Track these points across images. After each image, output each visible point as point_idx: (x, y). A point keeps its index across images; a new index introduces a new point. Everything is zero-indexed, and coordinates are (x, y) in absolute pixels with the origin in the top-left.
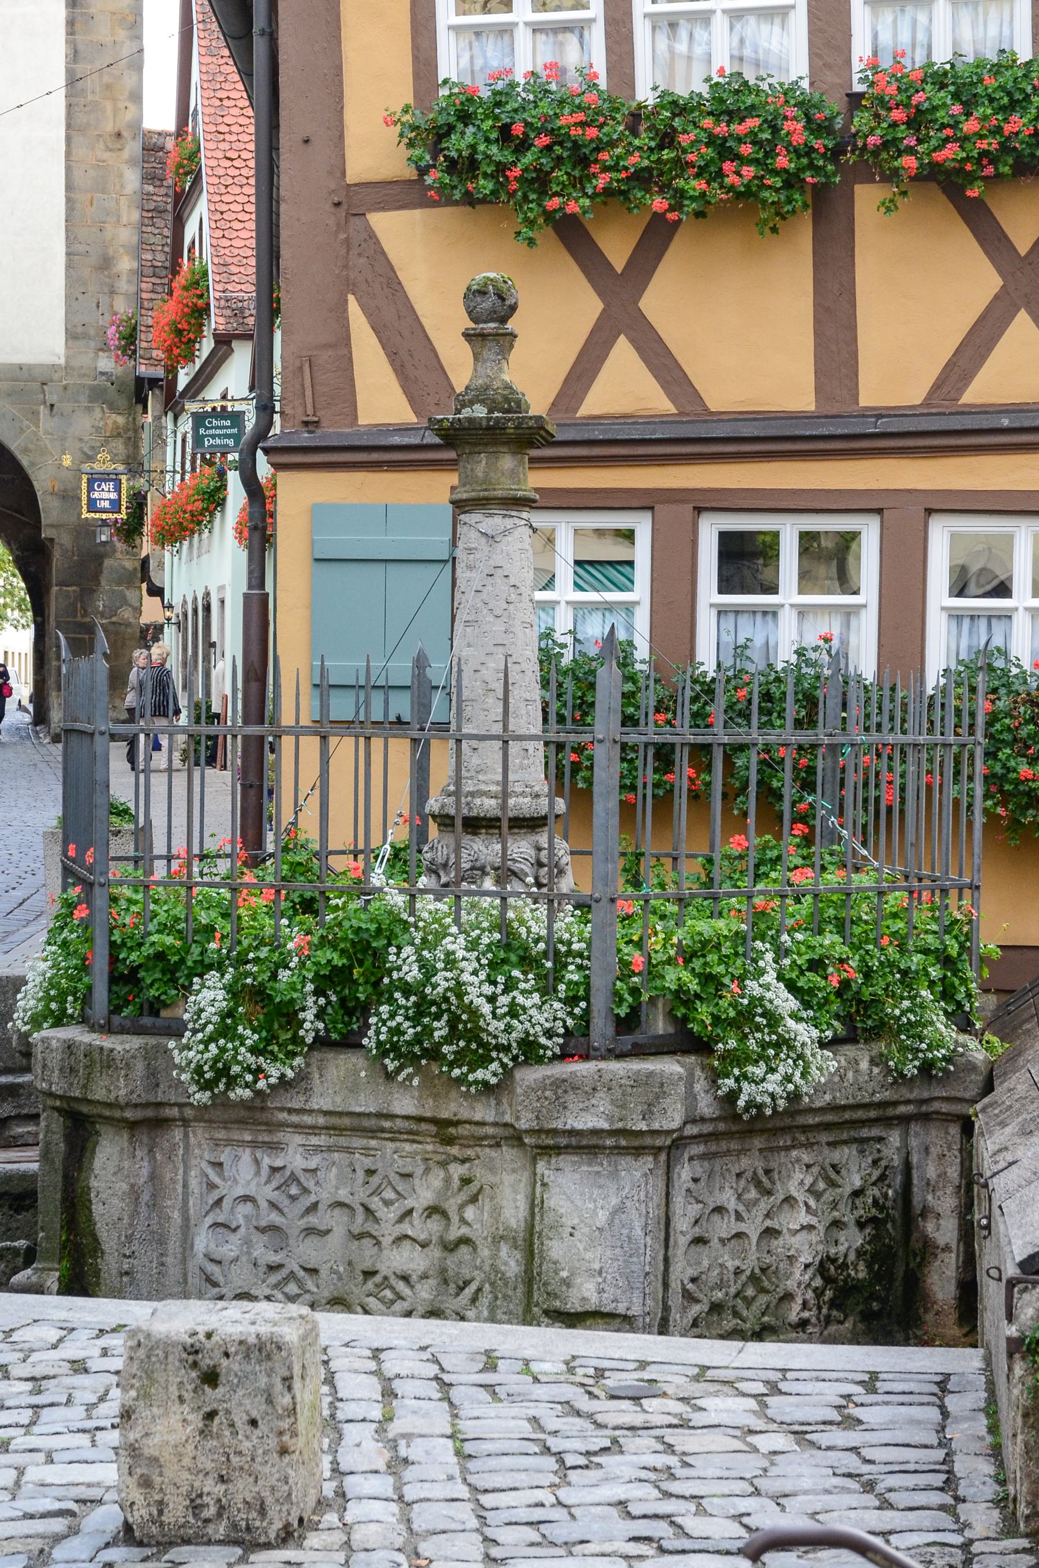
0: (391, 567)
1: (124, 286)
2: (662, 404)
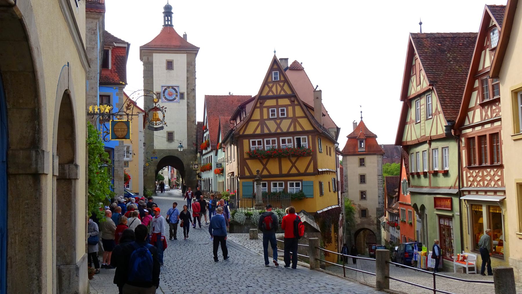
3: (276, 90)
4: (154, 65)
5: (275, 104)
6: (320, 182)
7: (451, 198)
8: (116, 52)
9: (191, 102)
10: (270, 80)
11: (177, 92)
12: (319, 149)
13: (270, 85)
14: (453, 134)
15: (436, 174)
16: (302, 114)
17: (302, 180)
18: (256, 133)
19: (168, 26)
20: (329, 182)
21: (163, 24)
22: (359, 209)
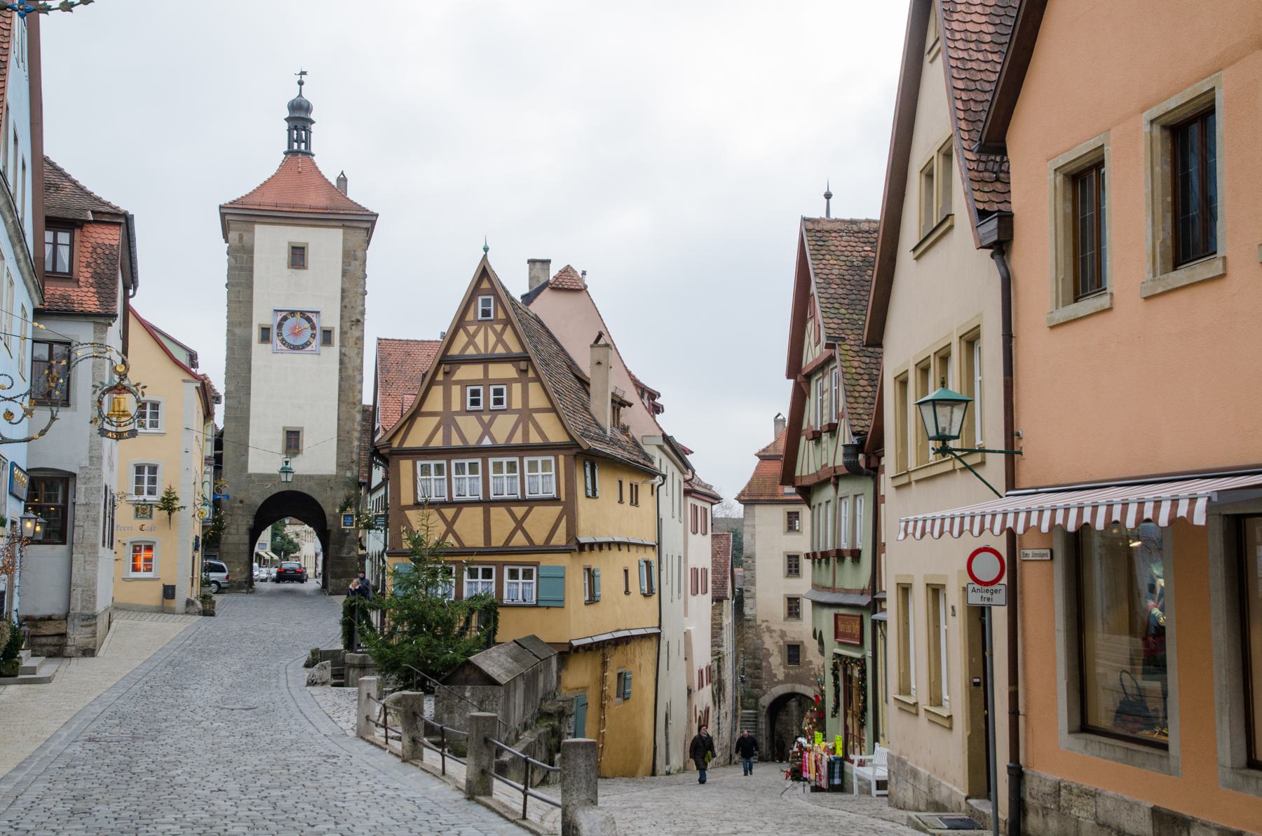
1: (356, 450)
3: (485, 341)
4: (257, 255)
5: (481, 377)
6: (589, 570)
7: (861, 617)
8: (97, 236)
9: (352, 352)
10: (470, 317)
11: (313, 327)
12: (586, 488)
13: (472, 329)
14: (863, 464)
15: (840, 555)
16: (541, 402)
17: (539, 563)
19: (300, 155)
20: (626, 571)
21: (286, 149)
22: (782, 644)
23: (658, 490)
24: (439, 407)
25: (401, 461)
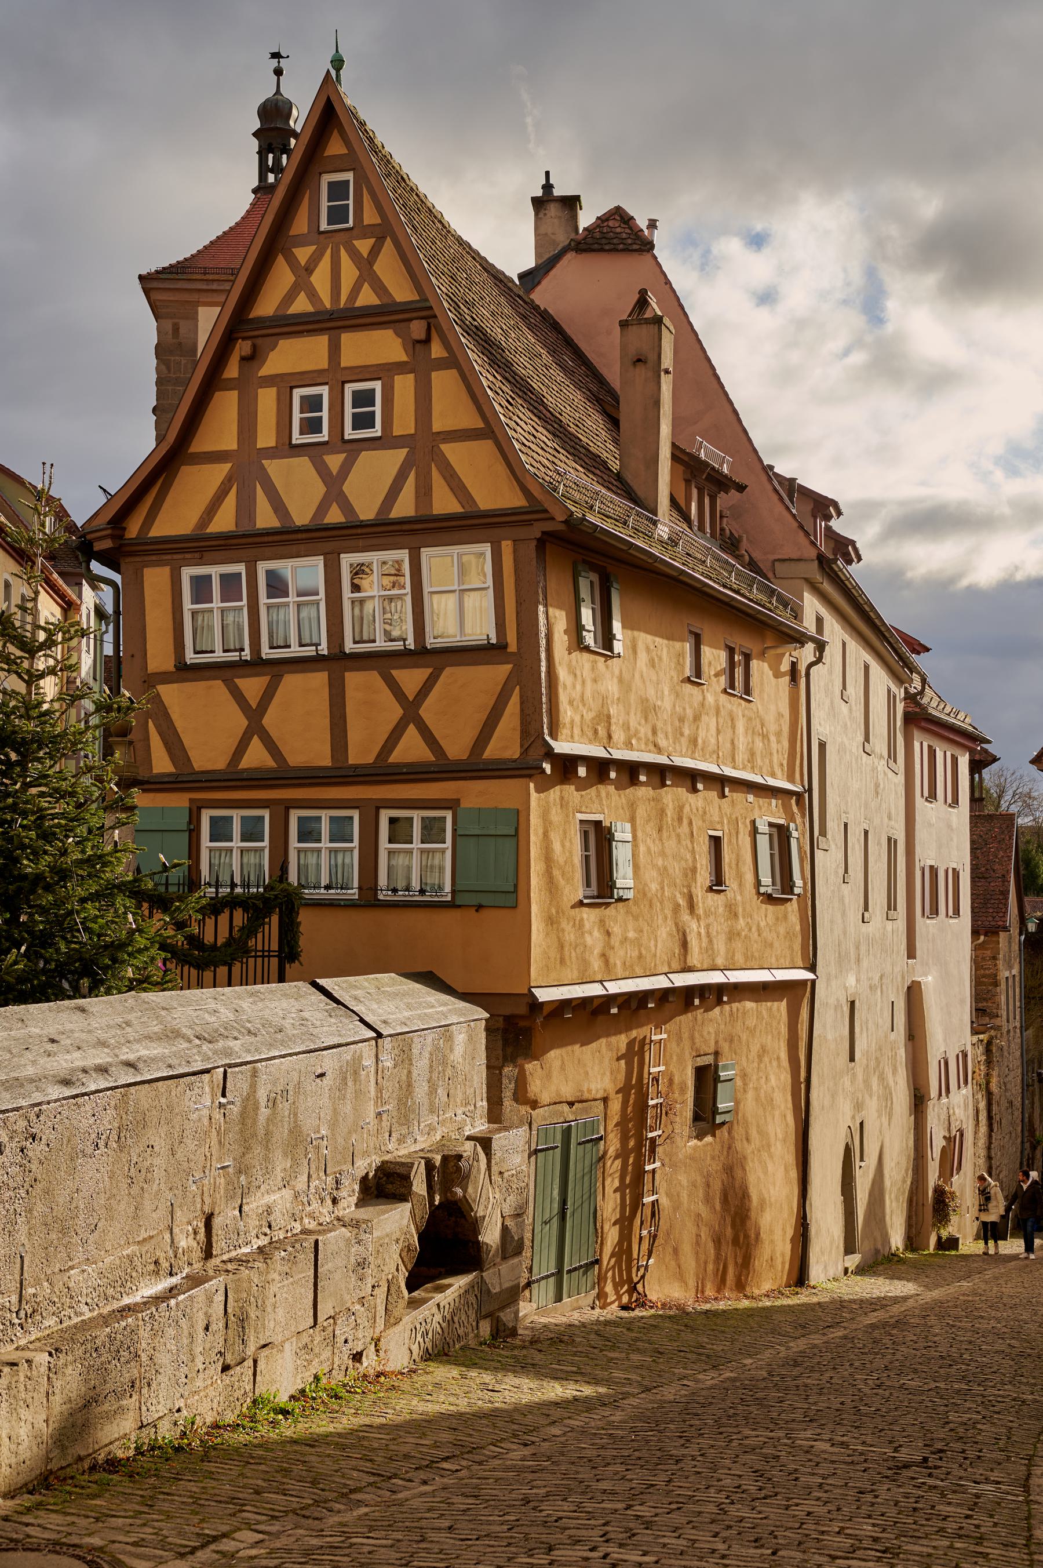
0: (165, 834)
2: (271, 763)
5: (322, 362)
10: (300, 225)
13: (303, 254)
18: (208, 531)
21: (255, 183)
23: (808, 675)
24: (230, 442)
25: (145, 570)
